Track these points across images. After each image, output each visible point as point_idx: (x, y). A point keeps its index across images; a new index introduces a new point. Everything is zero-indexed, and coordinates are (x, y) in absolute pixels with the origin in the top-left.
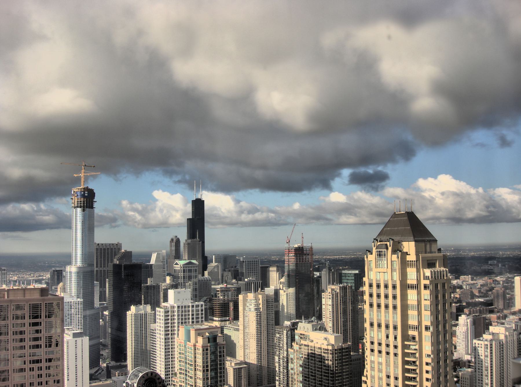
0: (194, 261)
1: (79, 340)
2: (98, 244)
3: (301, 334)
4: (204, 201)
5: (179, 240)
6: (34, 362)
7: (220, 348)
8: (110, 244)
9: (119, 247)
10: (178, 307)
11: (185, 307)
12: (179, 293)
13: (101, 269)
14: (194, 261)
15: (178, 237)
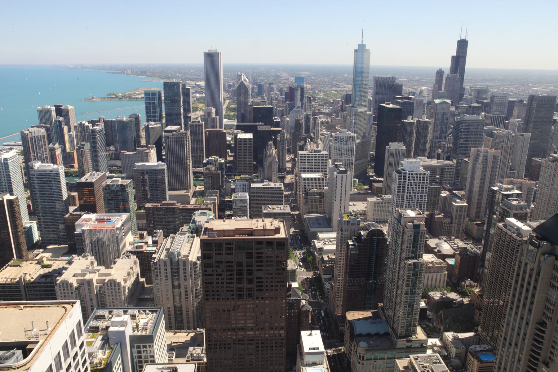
0: (449, 101)
1: (344, 175)
2: (378, 77)
3: (504, 209)
4: (467, 42)
5: (443, 72)
6: (269, 274)
7: (422, 233)
8: (387, 78)
9: (393, 80)
10: (409, 174)
11: (415, 174)
12: (411, 163)
13: (379, 96)
14: (449, 101)
15: (442, 70)
